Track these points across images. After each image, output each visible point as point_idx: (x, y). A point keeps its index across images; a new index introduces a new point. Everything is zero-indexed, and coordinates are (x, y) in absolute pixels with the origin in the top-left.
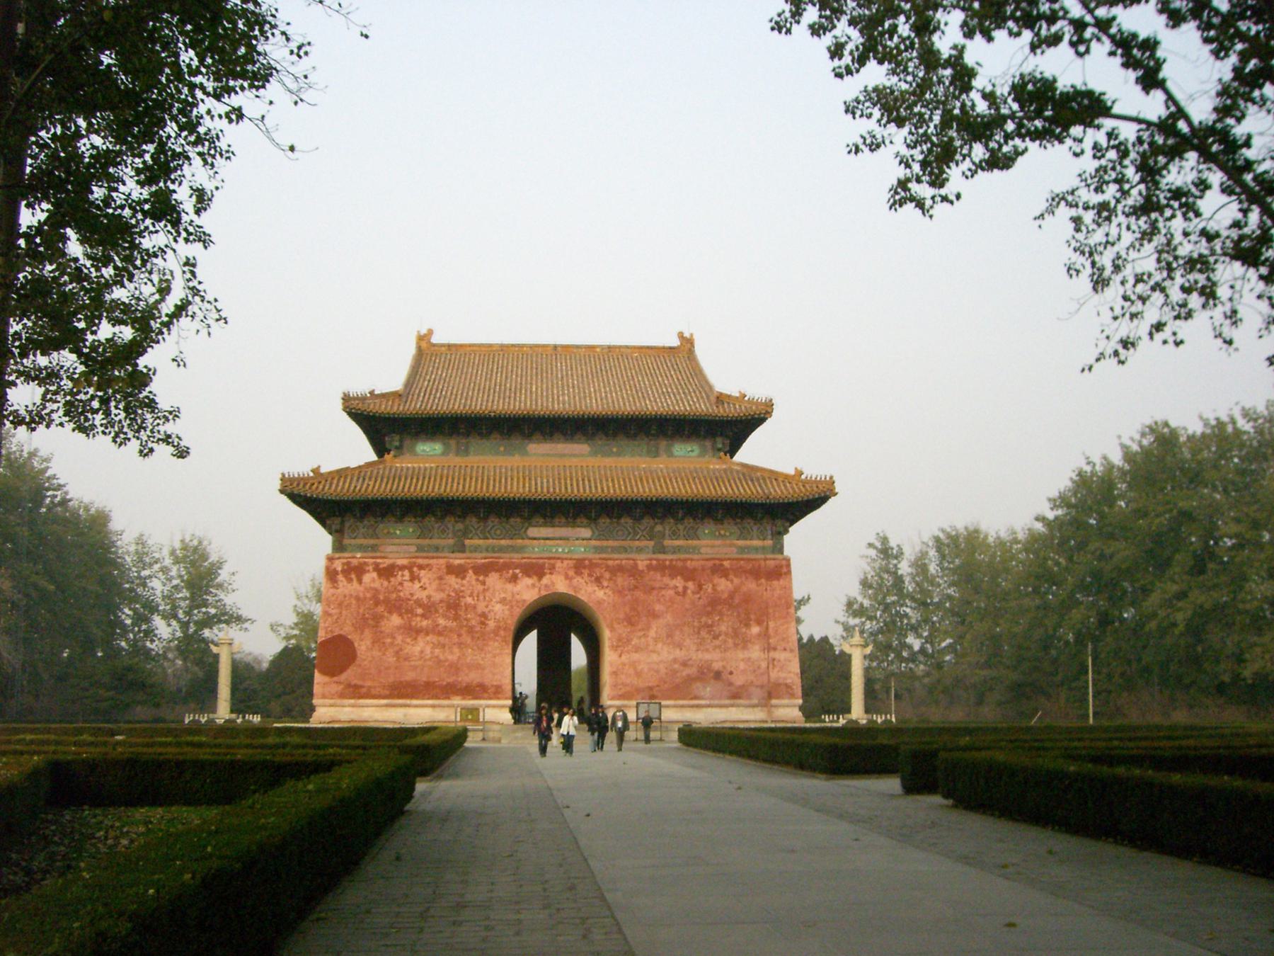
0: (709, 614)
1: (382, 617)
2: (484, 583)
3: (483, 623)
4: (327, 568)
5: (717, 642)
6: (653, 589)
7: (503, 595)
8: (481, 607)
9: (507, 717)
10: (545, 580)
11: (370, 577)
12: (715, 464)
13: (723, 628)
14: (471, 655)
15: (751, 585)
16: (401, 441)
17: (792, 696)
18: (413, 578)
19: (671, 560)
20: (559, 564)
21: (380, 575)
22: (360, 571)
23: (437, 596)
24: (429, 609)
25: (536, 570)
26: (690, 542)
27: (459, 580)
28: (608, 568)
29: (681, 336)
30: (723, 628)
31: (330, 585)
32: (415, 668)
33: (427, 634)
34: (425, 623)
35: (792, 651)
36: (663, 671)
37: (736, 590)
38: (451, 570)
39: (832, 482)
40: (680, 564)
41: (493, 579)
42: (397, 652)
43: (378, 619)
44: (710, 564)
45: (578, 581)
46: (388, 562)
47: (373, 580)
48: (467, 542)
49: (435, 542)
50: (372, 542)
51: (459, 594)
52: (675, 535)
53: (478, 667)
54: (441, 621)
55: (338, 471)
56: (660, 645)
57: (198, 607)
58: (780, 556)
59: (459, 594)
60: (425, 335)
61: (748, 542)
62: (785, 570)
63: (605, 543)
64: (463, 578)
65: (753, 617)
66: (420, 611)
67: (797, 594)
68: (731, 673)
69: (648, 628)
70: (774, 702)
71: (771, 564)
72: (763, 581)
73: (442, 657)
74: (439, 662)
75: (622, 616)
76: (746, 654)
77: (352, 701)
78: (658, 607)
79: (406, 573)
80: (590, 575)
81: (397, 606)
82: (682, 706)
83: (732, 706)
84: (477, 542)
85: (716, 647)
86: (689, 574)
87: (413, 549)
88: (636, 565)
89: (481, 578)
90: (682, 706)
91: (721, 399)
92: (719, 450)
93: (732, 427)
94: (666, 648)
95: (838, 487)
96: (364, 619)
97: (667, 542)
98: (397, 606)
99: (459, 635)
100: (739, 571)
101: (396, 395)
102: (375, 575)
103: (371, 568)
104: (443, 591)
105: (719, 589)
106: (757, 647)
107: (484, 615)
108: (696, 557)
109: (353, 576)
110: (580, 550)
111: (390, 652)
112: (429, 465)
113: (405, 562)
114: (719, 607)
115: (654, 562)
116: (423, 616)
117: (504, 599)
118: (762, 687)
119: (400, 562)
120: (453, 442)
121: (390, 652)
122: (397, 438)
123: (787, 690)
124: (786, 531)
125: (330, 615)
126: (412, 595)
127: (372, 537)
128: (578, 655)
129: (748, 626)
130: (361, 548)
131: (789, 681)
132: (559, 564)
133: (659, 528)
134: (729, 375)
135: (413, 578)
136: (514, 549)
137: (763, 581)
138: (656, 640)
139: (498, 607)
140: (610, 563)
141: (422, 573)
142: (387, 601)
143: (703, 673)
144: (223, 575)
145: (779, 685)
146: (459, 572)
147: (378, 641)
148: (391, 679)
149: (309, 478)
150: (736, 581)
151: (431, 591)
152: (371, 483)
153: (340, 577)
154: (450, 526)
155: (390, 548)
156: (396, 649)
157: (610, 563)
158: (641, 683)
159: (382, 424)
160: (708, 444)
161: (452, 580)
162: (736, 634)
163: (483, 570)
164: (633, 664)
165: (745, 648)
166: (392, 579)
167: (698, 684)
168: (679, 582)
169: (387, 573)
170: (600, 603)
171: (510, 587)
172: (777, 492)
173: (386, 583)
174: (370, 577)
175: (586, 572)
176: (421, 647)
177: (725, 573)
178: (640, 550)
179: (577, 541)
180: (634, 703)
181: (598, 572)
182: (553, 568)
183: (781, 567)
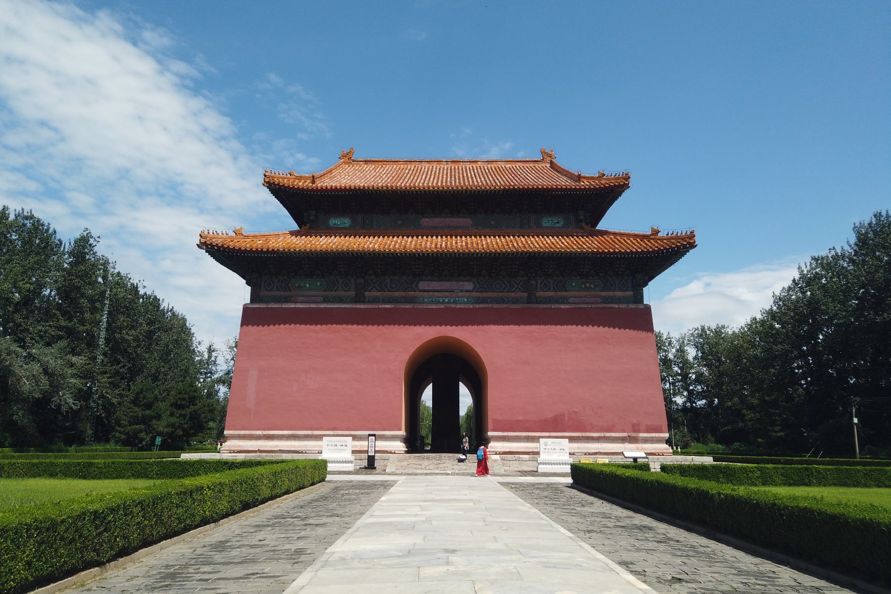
9: (400, 446)
26: (559, 293)
48: (367, 294)
49: (341, 293)
61: (611, 294)
63: (485, 295)
84: (374, 293)
92: (581, 221)
95: (698, 240)
124: (646, 284)
128: (466, 400)
133: (533, 282)
154: (352, 281)
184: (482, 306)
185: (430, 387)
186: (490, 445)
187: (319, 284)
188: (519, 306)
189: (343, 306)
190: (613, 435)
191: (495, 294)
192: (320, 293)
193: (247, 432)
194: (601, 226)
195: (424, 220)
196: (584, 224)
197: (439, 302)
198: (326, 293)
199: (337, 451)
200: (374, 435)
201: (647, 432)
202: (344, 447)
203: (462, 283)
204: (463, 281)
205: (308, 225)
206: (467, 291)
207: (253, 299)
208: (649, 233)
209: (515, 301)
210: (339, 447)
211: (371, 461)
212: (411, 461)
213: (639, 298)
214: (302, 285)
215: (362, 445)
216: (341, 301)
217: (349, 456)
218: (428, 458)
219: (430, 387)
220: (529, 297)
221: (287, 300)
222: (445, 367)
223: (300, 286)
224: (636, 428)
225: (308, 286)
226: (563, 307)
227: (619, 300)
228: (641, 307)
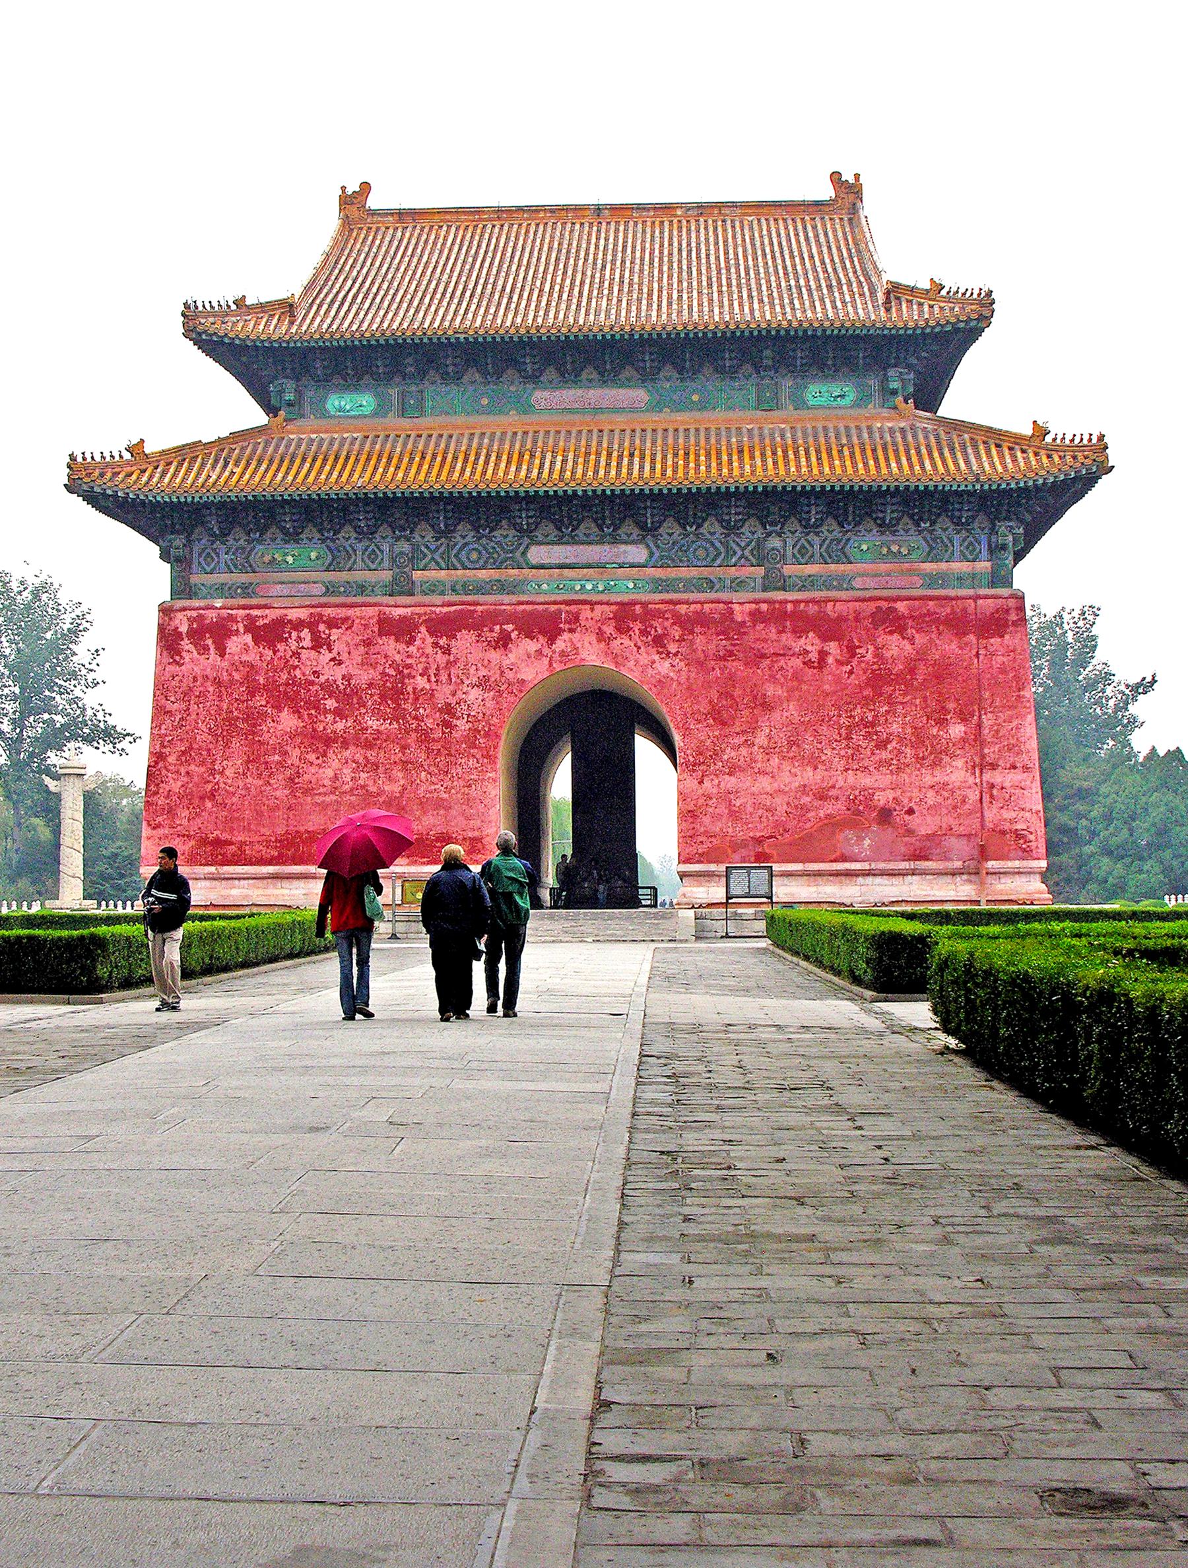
0: (867, 702)
1: (263, 716)
2: (447, 651)
3: (447, 724)
4: (161, 629)
5: (885, 755)
6: (763, 656)
7: (483, 672)
8: (443, 694)
10: (560, 644)
11: (239, 643)
12: (884, 422)
13: (895, 728)
14: (425, 784)
15: (948, 646)
16: (299, 393)
17: (1027, 854)
18: (318, 643)
19: (796, 602)
20: (585, 612)
21: (256, 641)
22: (221, 632)
23: (363, 677)
24: (349, 698)
25: (545, 625)
27: (402, 647)
28: (679, 620)
29: (836, 177)
30: (895, 728)
31: (167, 659)
32: (324, 806)
33: (345, 745)
34: (340, 726)
35: (1026, 769)
36: (782, 808)
37: (921, 656)
38: (387, 627)
39: (1101, 446)
40: (813, 609)
41: (464, 643)
42: (291, 779)
43: (254, 719)
44: (871, 607)
45: (621, 643)
46: (272, 614)
47: (246, 649)
48: (417, 575)
50: (244, 578)
51: (403, 672)
52: (804, 556)
53: (440, 804)
54: (373, 723)
55: (180, 449)
56: (775, 761)
57: (38, 712)
58: (1004, 592)
59: (403, 672)
61: (943, 566)
62: (1013, 617)
63: (672, 573)
64: (411, 642)
65: (951, 706)
66: (331, 704)
67: (1127, 673)
68: (911, 812)
69: (754, 728)
70: (991, 864)
71: (987, 606)
72: (972, 638)
73: (373, 789)
74: (368, 797)
75: (704, 707)
76: (940, 776)
77: (212, 869)
78: (771, 690)
79: (305, 633)
80: (644, 633)
81: (290, 695)
82: (819, 874)
83: (913, 873)
85: (880, 764)
86: (829, 629)
87: (319, 589)
88: (731, 612)
89: (443, 641)
90: (819, 874)
91: (895, 292)
93: (924, 348)
94: (786, 766)
95: (1114, 456)
96: (231, 721)
98: (290, 695)
99: (404, 748)
100: (925, 621)
101: (287, 307)
102: (248, 638)
103: (241, 626)
104: (374, 666)
105: (888, 654)
106: (960, 763)
107: (449, 709)
108: (843, 595)
109: (209, 642)
110: (626, 588)
111: (278, 780)
113: (303, 614)
114: (888, 689)
115: (764, 607)
116: (339, 713)
117: (486, 679)
118: (969, 836)
119: (293, 614)
121: (278, 780)
122: (290, 385)
123: (1019, 843)
125: (169, 713)
126: (316, 673)
129: (942, 723)
130: (221, 590)
131: (1019, 827)
132: (585, 612)
133: (775, 542)
134: (913, 249)
135: (318, 643)
136: (503, 587)
137: (972, 638)
138: (768, 751)
139: (474, 694)
140: (683, 609)
141: (335, 634)
142: (270, 688)
143: (858, 813)
144: (82, 652)
145: (1003, 833)
146: (403, 630)
147: (255, 759)
148: (281, 830)
149: (123, 464)
150: (920, 639)
151: (351, 666)
152: (238, 470)
153: (186, 644)
155: (279, 589)
156: (288, 773)
157: (683, 609)
158: (739, 832)
159: (265, 357)
161: (390, 646)
162: (919, 738)
163: (445, 627)
164: (727, 796)
165: (936, 764)
166: (280, 647)
167: (849, 833)
168: (810, 643)
169: (269, 634)
170: (661, 683)
171: (494, 656)
172: (995, 468)
173: (268, 654)
174: (239, 643)
175: (637, 627)
176: (334, 769)
177: (897, 624)
178: (738, 584)
179: (622, 568)
180: (722, 868)
181: (658, 626)
182: (576, 618)
183: (1007, 611)
187: (313, 555)
191: (694, 572)
192: (314, 576)
198: (328, 576)
203: (623, 547)
205: (282, 413)
206: (632, 566)
207: (176, 593)
214: (278, 557)
225: (290, 559)
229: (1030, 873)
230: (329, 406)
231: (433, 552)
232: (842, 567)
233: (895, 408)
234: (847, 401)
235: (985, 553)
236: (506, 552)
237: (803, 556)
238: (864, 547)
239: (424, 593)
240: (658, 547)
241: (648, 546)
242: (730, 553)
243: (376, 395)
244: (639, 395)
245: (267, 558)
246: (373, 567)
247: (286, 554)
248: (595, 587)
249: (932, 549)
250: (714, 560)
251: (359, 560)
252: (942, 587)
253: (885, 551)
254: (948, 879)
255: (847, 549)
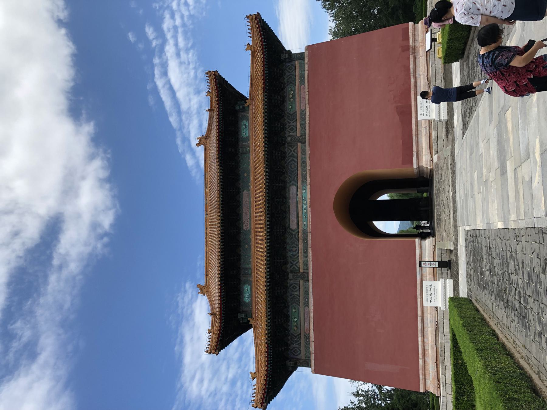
9: (428, 243)
16: (242, 312)
26: (297, 118)
48: (301, 271)
52: (294, 129)
60: (201, 289)
61: (297, 78)
92: (244, 107)
97: (298, 134)
112: (256, 295)
120: (243, 278)
122: (240, 315)
127: (300, 338)
133: (289, 139)
136: (305, 238)
154: (291, 283)
160: (241, 115)
184: (308, 178)
185: (376, 223)
186: (424, 166)
187: (294, 310)
188: (308, 149)
189: (311, 290)
190: (412, 66)
193: (421, 372)
194: (247, 94)
195: (244, 228)
196: (246, 105)
197: (306, 213)
199: (436, 294)
200: (420, 262)
201: (408, 39)
202: (432, 288)
203: (291, 195)
204: (289, 194)
205: (249, 319)
207: (308, 365)
208: (250, 52)
209: (304, 152)
210: (432, 292)
211: (442, 264)
212: (442, 230)
213: (300, 56)
215: (428, 271)
216: (307, 292)
217: (439, 284)
218: (439, 215)
219: (376, 223)
220: (301, 142)
221: (308, 337)
222: (360, 206)
223: (296, 326)
224: (406, 48)
225: (296, 320)
226: (308, 114)
227: (302, 70)
228: (306, 54)
229: (415, 35)
230: (248, 301)
231: (293, 265)
232: (298, 115)
233: (248, 106)
234: (247, 123)
235: (292, 63)
236: (292, 238)
237: (293, 129)
238: (290, 107)
239: (308, 269)
240: (291, 182)
241: (290, 185)
242: (292, 156)
243: (244, 284)
244: (245, 193)
245: (295, 328)
246: (298, 288)
247: (294, 321)
248: (305, 205)
249: (291, 83)
250: (295, 161)
251: (296, 293)
252: (304, 77)
253: (292, 100)
254: (417, 60)
255: (291, 113)
